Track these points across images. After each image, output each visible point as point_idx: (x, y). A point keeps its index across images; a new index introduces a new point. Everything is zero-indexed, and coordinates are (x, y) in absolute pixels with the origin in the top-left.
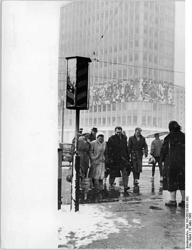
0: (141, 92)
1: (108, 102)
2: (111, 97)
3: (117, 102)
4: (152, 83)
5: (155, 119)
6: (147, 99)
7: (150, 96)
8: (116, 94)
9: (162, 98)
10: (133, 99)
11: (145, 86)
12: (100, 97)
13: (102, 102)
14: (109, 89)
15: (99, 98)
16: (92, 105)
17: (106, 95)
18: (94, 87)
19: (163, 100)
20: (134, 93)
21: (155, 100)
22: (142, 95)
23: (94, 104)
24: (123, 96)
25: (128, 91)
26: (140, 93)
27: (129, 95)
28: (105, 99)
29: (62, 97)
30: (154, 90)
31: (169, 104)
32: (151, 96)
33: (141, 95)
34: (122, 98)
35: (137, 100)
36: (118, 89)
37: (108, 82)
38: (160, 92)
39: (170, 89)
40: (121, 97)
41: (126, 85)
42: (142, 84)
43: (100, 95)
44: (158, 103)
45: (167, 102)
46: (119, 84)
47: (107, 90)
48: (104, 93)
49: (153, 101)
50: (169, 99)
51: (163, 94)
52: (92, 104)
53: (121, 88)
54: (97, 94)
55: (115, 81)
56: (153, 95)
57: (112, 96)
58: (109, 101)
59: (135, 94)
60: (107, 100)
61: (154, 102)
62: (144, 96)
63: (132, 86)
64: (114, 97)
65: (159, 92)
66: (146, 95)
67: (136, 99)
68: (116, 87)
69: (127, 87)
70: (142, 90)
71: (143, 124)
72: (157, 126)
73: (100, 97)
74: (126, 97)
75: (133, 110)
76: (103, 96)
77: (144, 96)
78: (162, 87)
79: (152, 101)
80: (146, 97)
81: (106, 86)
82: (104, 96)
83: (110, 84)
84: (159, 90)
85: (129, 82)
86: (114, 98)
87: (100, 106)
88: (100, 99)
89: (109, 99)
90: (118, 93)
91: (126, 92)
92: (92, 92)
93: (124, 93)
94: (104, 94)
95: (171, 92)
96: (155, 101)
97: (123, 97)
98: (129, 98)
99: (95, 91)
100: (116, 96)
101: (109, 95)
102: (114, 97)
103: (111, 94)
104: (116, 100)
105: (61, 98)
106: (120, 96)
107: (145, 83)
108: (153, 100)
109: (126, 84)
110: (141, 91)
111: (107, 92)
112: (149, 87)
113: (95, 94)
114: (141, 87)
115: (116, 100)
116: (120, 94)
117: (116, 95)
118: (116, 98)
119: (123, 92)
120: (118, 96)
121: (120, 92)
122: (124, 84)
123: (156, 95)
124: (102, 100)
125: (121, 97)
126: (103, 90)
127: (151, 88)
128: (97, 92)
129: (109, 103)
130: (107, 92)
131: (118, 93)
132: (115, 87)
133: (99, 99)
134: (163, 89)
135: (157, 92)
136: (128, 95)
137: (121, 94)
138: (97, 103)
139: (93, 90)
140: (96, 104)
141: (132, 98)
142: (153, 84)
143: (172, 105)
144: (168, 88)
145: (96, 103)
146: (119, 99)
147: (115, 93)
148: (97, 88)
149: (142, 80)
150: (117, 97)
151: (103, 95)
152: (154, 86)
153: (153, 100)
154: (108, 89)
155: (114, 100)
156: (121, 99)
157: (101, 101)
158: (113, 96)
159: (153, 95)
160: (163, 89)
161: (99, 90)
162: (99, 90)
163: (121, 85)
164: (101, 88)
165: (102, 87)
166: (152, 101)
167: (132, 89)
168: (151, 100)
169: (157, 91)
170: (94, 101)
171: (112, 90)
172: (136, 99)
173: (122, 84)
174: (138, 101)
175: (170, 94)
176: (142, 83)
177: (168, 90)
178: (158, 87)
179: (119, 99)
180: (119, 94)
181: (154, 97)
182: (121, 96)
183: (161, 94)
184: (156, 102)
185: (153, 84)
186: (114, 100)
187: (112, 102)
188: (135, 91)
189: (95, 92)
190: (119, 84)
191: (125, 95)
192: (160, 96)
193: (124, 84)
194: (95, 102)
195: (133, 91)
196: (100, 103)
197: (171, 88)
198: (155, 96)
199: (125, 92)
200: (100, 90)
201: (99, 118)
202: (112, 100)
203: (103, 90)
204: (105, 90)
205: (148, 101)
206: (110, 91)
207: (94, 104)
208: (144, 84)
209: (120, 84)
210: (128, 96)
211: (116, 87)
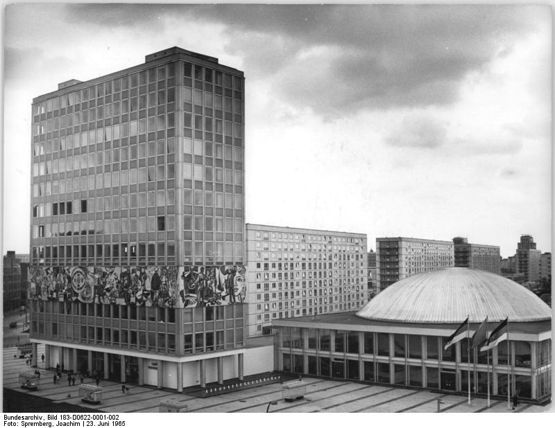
0: (182, 293)
1: (121, 302)
3: (138, 304)
4: (202, 269)
5: (210, 336)
6: (192, 304)
7: (199, 295)
8: (137, 289)
9: (224, 294)
11: (188, 280)
12: (108, 290)
13: (111, 300)
15: (105, 291)
17: (117, 287)
18: (95, 269)
19: (224, 298)
23: (97, 300)
24: (148, 294)
25: (159, 286)
26: (179, 293)
27: (159, 294)
28: (118, 295)
29: (38, 278)
30: (206, 283)
31: (238, 303)
32: (202, 296)
33: (181, 298)
34: (146, 297)
37: (122, 264)
38: (218, 284)
39: (237, 274)
40: (146, 295)
42: (183, 276)
43: (106, 287)
44: (216, 305)
45: (233, 300)
46: (140, 270)
47: (119, 278)
48: (115, 282)
49: (206, 303)
50: (236, 294)
52: (92, 301)
53: (145, 278)
54: (102, 283)
55: (134, 264)
56: (205, 294)
58: (124, 300)
59: (170, 295)
60: (120, 297)
61: (207, 305)
63: (164, 279)
64: (133, 293)
65: (215, 285)
66: (191, 295)
67: (172, 305)
68: (136, 275)
69: (156, 281)
70: (182, 287)
71: (186, 351)
72: (215, 348)
74: (155, 297)
76: (113, 290)
78: (221, 274)
79: (203, 304)
81: (118, 271)
82: (115, 288)
83: (125, 268)
84: (216, 282)
85: (160, 270)
86: (132, 295)
87: (108, 306)
88: (108, 294)
92: (93, 277)
93: (150, 289)
94: (115, 286)
95: (239, 280)
97: (149, 297)
98: (160, 300)
99: (97, 276)
100: (136, 293)
102: (133, 293)
103: (127, 286)
104: (136, 299)
105: (36, 282)
106: (143, 294)
108: (206, 301)
109: (154, 272)
110: (181, 290)
112: (196, 278)
113: (98, 283)
114: (181, 282)
115: (136, 299)
116: (143, 291)
117: (137, 290)
119: (148, 287)
120: (140, 293)
121: (144, 285)
123: (212, 291)
125: (146, 295)
126: (112, 277)
127: (201, 280)
129: (125, 304)
130: (119, 282)
131: (139, 287)
132: (134, 275)
133: (105, 294)
134: (224, 278)
135: (213, 285)
136: (157, 294)
137: (146, 291)
138: (102, 301)
139: (94, 274)
140: (101, 303)
141: (166, 301)
143: (241, 304)
144: (233, 272)
145: (99, 300)
146: (142, 299)
147: (135, 287)
148: (100, 271)
149: (182, 270)
151: (113, 287)
153: (206, 301)
155: (133, 300)
156: (144, 299)
158: (131, 291)
159: (205, 294)
160: (224, 278)
161: (104, 275)
163: (145, 273)
164: (108, 273)
165: (110, 271)
166: (203, 304)
171: (130, 281)
172: (172, 305)
173: (147, 271)
175: (239, 283)
176: (182, 274)
177: (235, 277)
178: (215, 275)
179: (142, 299)
181: (207, 296)
183: (220, 288)
185: (204, 273)
186: (133, 300)
187: (128, 300)
188: (170, 289)
189: (99, 279)
190: (140, 270)
191: (153, 294)
192: (218, 291)
193: (150, 272)
194: (99, 298)
196: (107, 302)
197: (239, 272)
198: (210, 293)
199: (152, 287)
201: (107, 329)
206: (126, 282)
207: (97, 300)
208: (186, 276)
209: (143, 270)
211: (136, 275)
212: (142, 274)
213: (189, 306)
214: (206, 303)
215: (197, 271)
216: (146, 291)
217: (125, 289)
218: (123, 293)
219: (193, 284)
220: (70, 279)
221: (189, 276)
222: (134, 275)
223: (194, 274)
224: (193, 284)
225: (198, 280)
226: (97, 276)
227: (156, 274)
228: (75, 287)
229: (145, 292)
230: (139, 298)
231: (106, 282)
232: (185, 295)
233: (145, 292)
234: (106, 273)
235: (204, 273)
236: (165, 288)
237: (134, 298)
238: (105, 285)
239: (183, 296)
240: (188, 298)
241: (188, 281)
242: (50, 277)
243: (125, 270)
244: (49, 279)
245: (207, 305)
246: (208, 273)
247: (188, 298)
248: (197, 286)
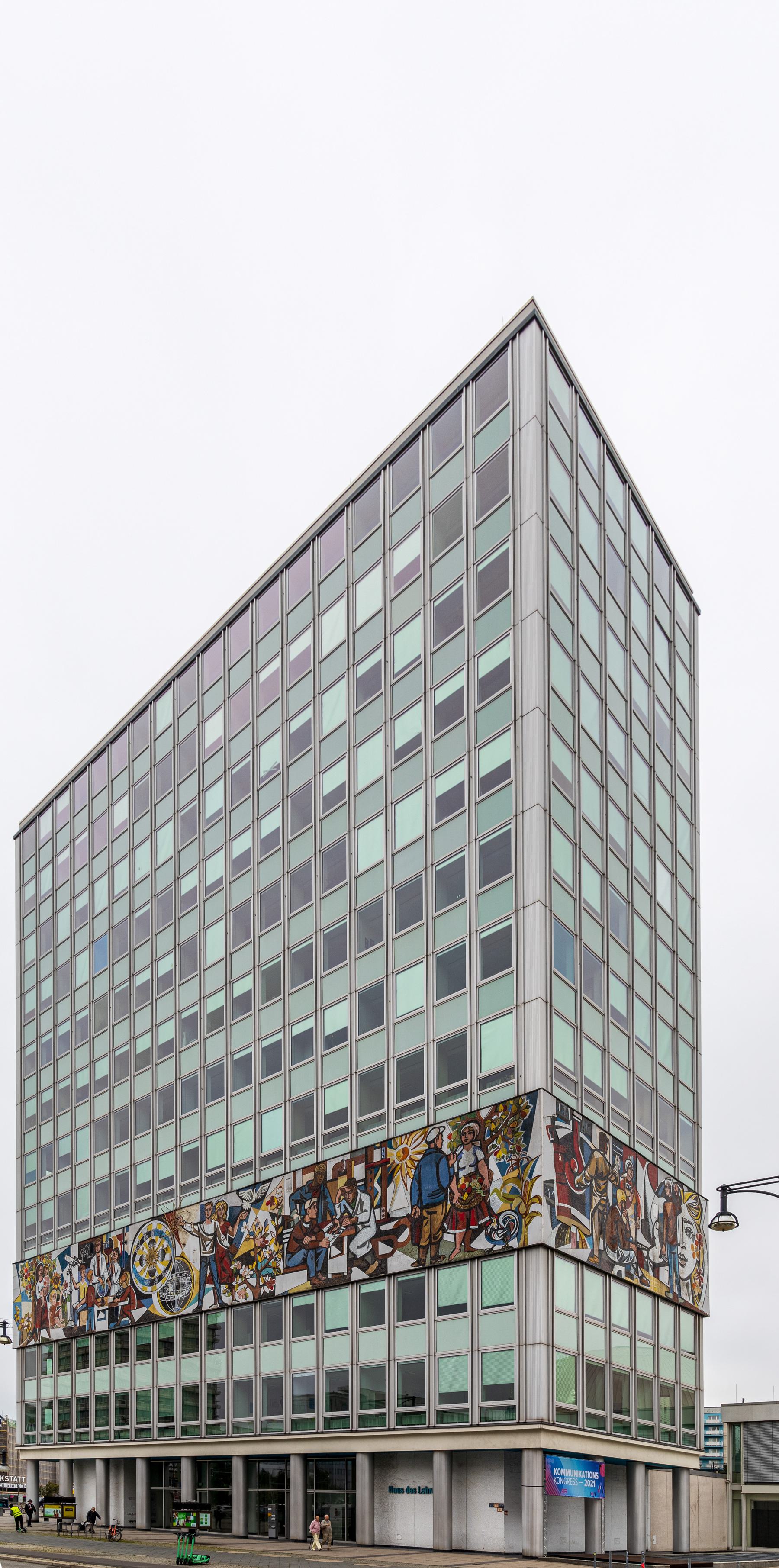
2: (315, 1247)
8: (354, 1225)
10: (481, 1243)
12: (247, 1259)
14: (302, 1202)
16: (200, 1307)
17: (279, 1239)
20: (485, 1199)
24: (397, 1231)
34: (389, 1243)
35: (514, 1243)
36: (365, 1198)
41: (425, 1154)
48: (271, 1228)
51: (656, 1232)
53: (388, 1179)
54: (226, 1243)
57: (323, 1244)
60: (288, 1270)
62: (564, 1219)
64: (339, 1244)
67: (505, 1239)
68: (352, 1182)
73: (247, 1259)
76: (265, 1253)
82: (273, 1247)
85: (448, 1131)
86: (335, 1251)
88: (246, 1271)
89: (305, 1260)
90: (363, 1217)
91: (426, 1200)
98: (448, 1237)
99: (209, 1228)
100: (351, 1239)
101: (299, 1241)
103: (316, 1229)
104: (352, 1261)
106: (379, 1235)
109: (424, 1147)
111: (287, 1221)
113: (215, 1244)
116: (379, 1223)
117: (354, 1228)
118: (353, 1247)
122: (405, 1151)
124: (258, 1273)
125: (389, 1239)
126: (263, 1215)
128: (225, 1233)
131: (363, 1217)
137: (388, 1219)
139: (201, 1222)
141: (476, 1233)
146: (374, 1251)
147: (347, 1222)
150: (360, 1245)
151: (265, 1245)
154: (297, 1199)
156: (383, 1249)
157: (253, 1281)
161: (235, 1216)
162: (235, 1216)
163: (385, 1161)
164: (247, 1206)
167: (468, 1177)
170: (207, 1286)
174: (519, 1250)
179: (374, 1251)
180: (372, 1223)
182: (388, 1232)
186: (337, 1265)
189: (215, 1234)
195: (475, 1183)
199: (418, 1201)
200: (243, 1216)
202: (325, 1265)
203: (263, 1215)
204: (273, 1216)
206: (312, 1213)
210: (437, 1225)
212: (371, 1168)
216: (388, 1219)
217: (307, 1240)
218: (299, 1256)
220: (125, 1261)
222: (342, 1181)
226: (209, 1228)
227: (433, 1151)
228: (142, 1281)
229: (390, 1226)
230: (360, 1253)
231: (240, 1235)
233: (390, 1226)
234: (242, 1209)
236: (470, 1190)
237: (344, 1258)
238: (237, 1250)
239: (551, 1205)
240: (564, 1219)
242: (70, 1273)
243: (310, 1176)
244: (67, 1279)
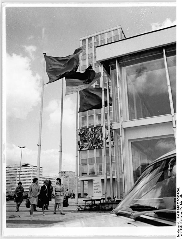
6: (85, 148)
21: (97, 146)
22: (79, 145)
30: (95, 136)
32: (92, 143)
42: (80, 134)
49: (94, 147)
56: (94, 141)
61: (95, 148)
65: (102, 136)
66: (84, 143)
75: (82, 159)
77: (82, 145)
80: (84, 146)
96: (98, 147)
107: (83, 132)
108: (94, 146)
112: (88, 134)
127: (91, 135)
135: (100, 137)
142: (94, 129)
152: (96, 132)
153: (94, 146)
159: (94, 141)
168: (91, 147)
169: (99, 135)
176: (79, 133)
178: (101, 131)
181: (95, 143)
184: (99, 147)
185: (94, 131)
205: (87, 148)
208: (81, 134)
213: (82, 149)
214: (94, 147)
215: (89, 130)
219: (87, 137)
221: (84, 134)
223: (87, 132)
224: (87, 137)
225: (89, 135)
232: (81, 143)
235: (94, 131)
241: (83, 136)
245: (95, 148)
246: (96, 130)
247: (83, 145)
248: (89, 138)
